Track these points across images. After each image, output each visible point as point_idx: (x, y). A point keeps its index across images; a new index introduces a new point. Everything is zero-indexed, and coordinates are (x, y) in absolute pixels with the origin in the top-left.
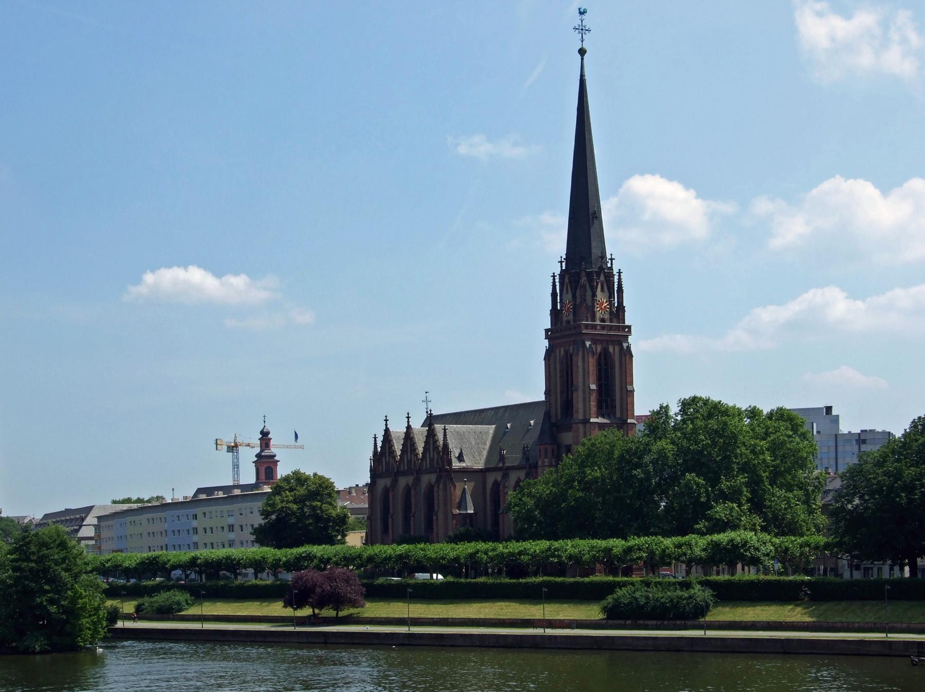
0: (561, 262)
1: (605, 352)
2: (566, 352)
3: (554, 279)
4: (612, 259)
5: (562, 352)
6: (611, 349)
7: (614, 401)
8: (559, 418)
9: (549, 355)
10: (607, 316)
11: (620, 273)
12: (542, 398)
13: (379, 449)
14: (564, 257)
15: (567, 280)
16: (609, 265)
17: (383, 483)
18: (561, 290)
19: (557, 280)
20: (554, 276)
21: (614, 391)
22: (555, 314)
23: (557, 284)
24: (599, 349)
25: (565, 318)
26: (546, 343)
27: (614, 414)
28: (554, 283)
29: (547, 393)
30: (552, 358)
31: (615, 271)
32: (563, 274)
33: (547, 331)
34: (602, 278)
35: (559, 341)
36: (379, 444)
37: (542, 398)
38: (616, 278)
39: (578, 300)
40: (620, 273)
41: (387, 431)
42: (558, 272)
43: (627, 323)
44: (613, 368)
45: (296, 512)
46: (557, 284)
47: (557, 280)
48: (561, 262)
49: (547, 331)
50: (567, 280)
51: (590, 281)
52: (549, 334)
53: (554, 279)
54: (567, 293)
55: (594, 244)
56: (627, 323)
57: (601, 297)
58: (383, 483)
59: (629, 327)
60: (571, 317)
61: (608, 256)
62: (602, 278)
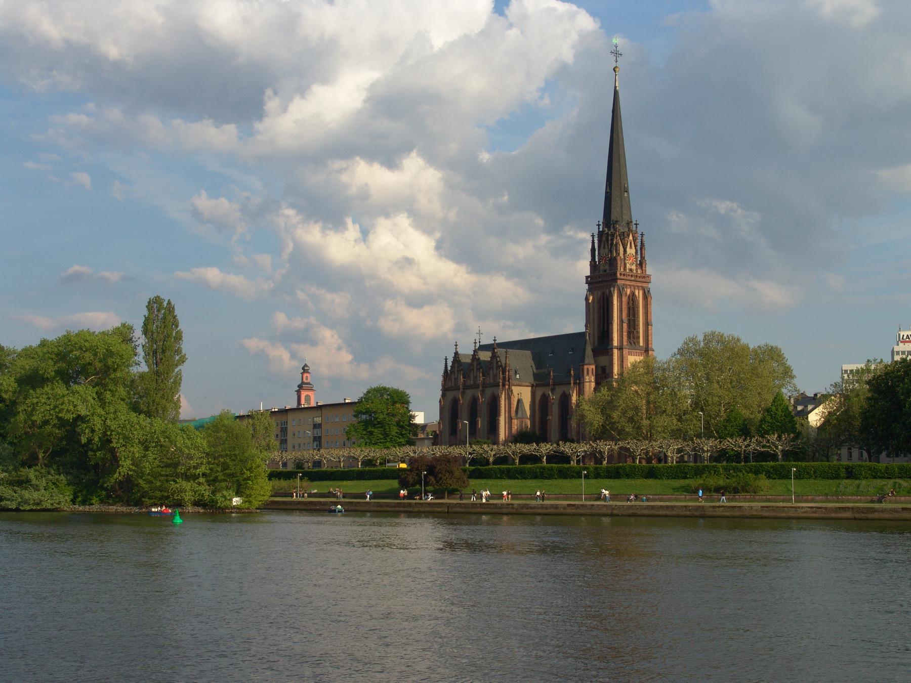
0: (599, 225)
1: (633, 294)
2: (603, 293)
6: (637, 293)
7: (638, 332)
10: (634, 267)
11: (642, 235)
13: (449, 368)
14: (601, 220)
15: (604, 238)
17: (450, 395)
18: (599, 247)
20: (593, 236)
21: (638, 325)
22: (593, 266)
25: (602, 268)
31: (639, 232)
32: (601, 234)
34: (631, 238)
36: (450, 364)
40: (642, 235)
41: (456, 354)
43: (648, 273)
45: (380, 414)
49: (587, 277)
50: (604, 238)
55: (625, 212)
56: (648, 273)
57: (631, 251)
58: (450, 395)
59: (649, 276)
60: (607, 267)
61: (634, 222)
62: (631, 238)
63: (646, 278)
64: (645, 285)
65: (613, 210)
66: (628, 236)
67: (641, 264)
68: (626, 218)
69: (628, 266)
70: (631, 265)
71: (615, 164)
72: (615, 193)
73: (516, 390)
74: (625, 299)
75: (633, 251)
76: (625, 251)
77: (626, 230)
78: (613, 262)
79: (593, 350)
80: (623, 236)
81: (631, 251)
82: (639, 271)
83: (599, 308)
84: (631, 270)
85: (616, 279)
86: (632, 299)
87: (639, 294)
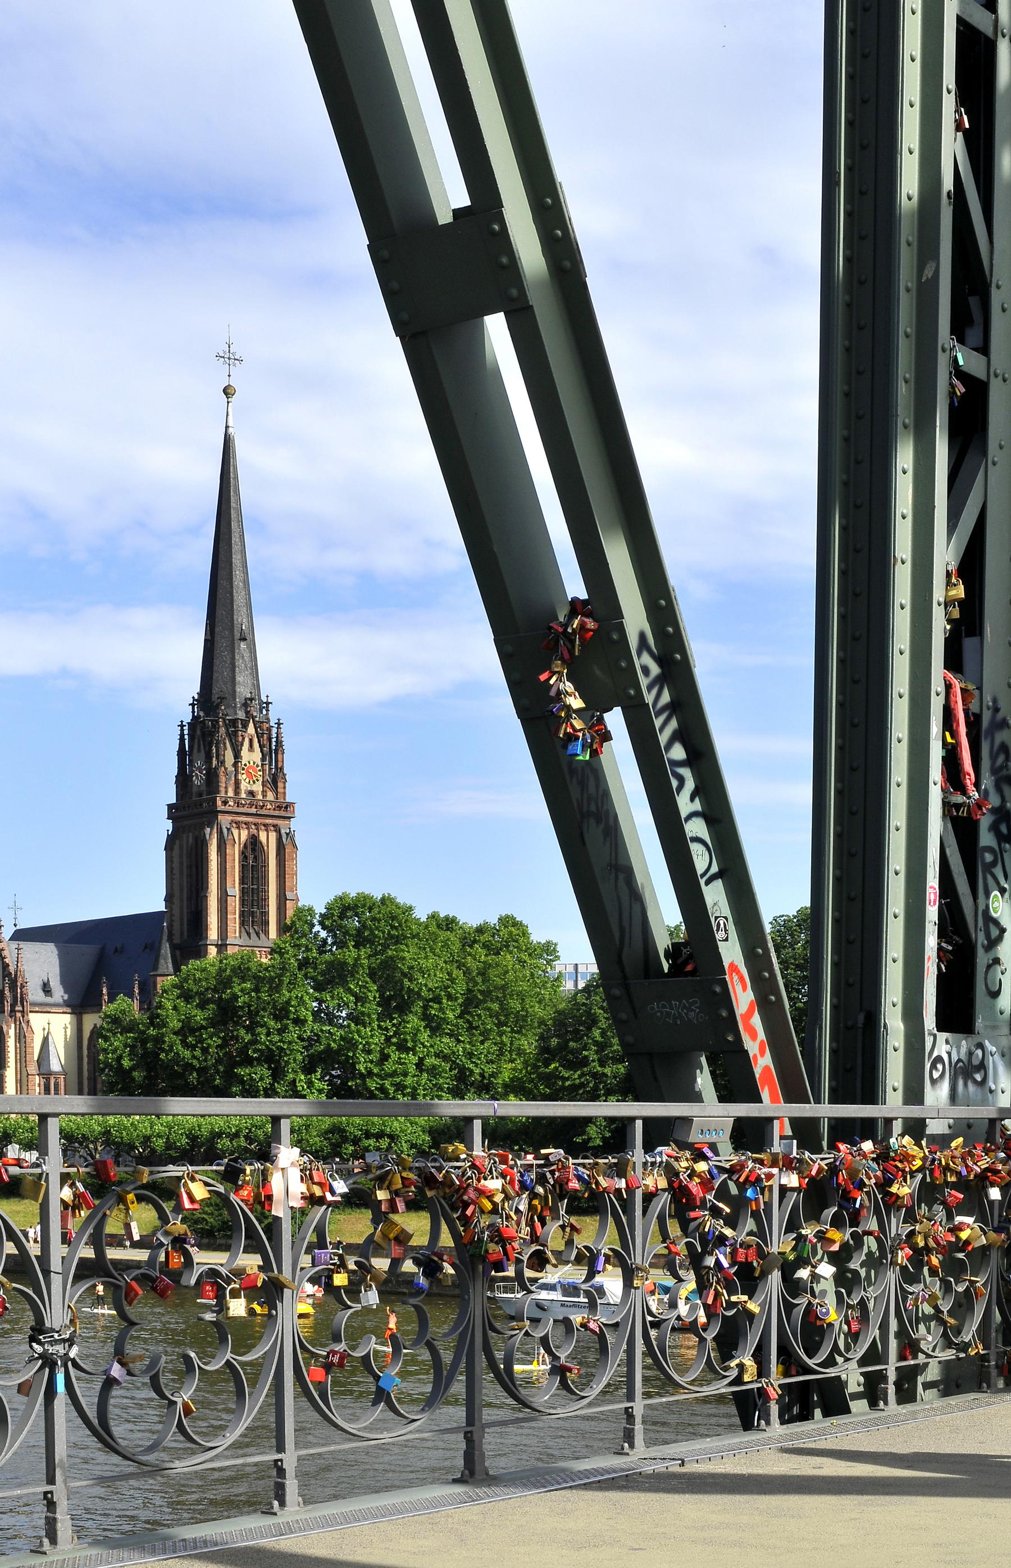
0: (193, 705)
2: (196, 839)
3: (182, 730)
4: (268, 703)
5: (191, 841)
6: (263, 836)
7: (266, 914)
8: (185, 936)
9: (171, 842)
10: (258, 788)
11: (279, 724)
12: (159, 905)
15: (198, 732)
16: (264, 712)
19: (186, 732)
20: (182, 726)
21: (266, 899)
23: (186, 737)
24: (244, 834)
26: (169, 825)
27: (267, 933)
28: (182, 735)
29: (168, 899)
30: (176, 847)
33: (170, 807)
34: (251, 729)
35: (186, 823)
37: (159, 905)
38: (274, 730)
39: (214, 762)
40: (279, 724)
42: (188, 718)
44: (266, 866)
46: (186, 737)
47: (186, 732)
48: (193, 705)
49: (170, 807)
50: (198, 732)
51: (233, 736)
52: (174, 812)
53: (182, 730)
54: (199, 751)
57: (251, 757)
59: (288, 806)
60: (204, 788)
62: (251, 729)
63: (285, 809)
64: (279, 822)
65: (215, 675)
66: (245, 726)
67: (275, 779)
68: (243, 691)
69: (244, 786)
70: (251, 784)
71: (222, 583)
72: (221, 644)
73: (37, 1021)
74: (234, 853)
75: (257, 756)
76: (237, 756)
77: (241, 715)
78: (212, 778)
79: (174, 948)
80: (235, 728)
81: (251, 757)
82: (270, 796)
83: (190, 867)
84: (251, 793)
85: (215, 813)
87: (269, 840)
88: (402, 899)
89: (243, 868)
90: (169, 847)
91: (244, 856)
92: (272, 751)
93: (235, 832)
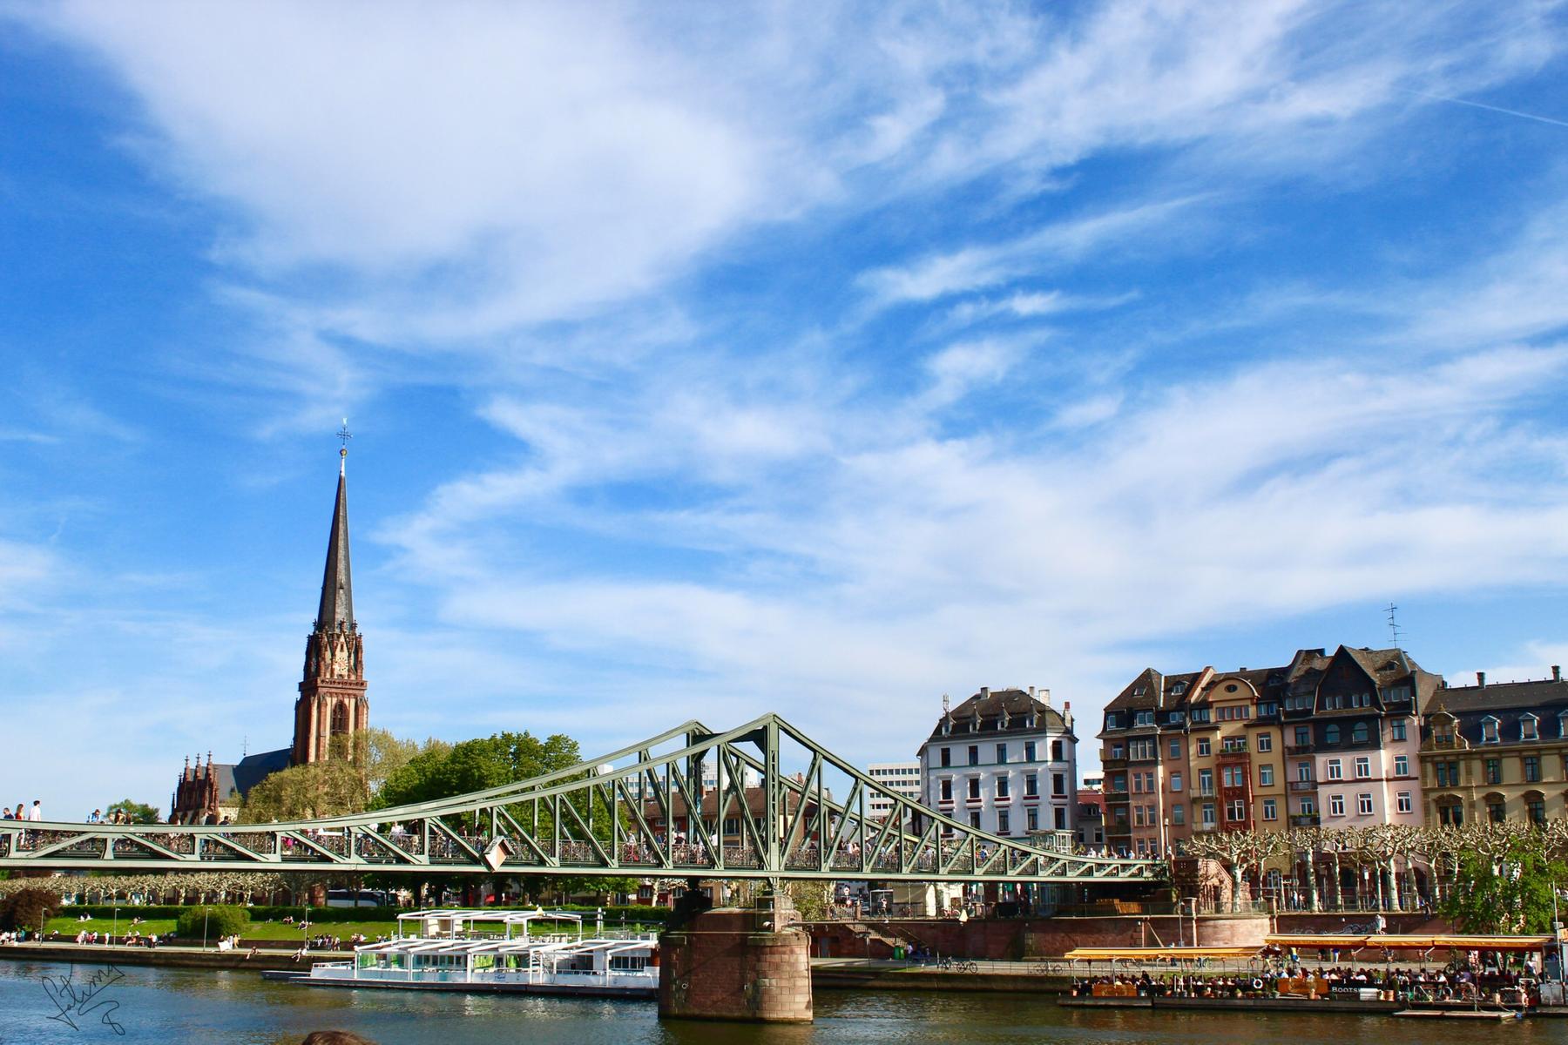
6: (346, 701)
10: (345, 673)
26: (298, 695)
34: (342, 639)
57: (342, 656)
62: (342, 639)
63: (361, 684)
67: (357, 666)
72: (330, 590)
75: (346, 653)
76: (333, 655)
77: (337, 631)
81: (342, 656)
82: (353, 677)
85: (317, 688)
86: (340, 708)
87: (350, 703)
88: (515, 730)
89: (334, 720)
90: (297, 708)
91: (334, 712)
92: (357, 650)
93: (328, 699)
